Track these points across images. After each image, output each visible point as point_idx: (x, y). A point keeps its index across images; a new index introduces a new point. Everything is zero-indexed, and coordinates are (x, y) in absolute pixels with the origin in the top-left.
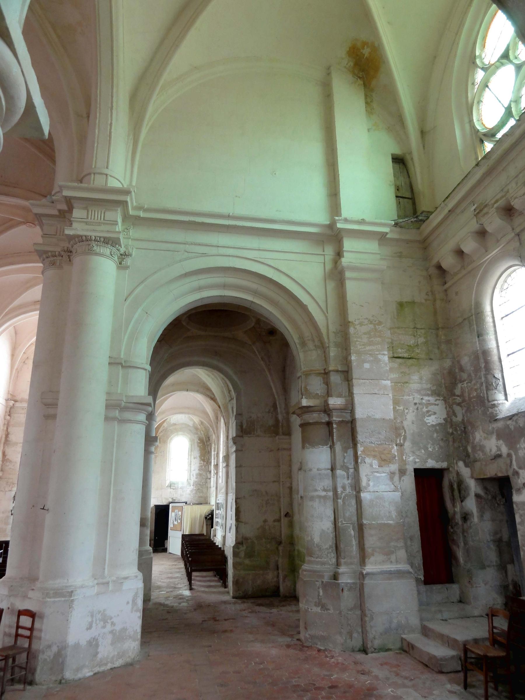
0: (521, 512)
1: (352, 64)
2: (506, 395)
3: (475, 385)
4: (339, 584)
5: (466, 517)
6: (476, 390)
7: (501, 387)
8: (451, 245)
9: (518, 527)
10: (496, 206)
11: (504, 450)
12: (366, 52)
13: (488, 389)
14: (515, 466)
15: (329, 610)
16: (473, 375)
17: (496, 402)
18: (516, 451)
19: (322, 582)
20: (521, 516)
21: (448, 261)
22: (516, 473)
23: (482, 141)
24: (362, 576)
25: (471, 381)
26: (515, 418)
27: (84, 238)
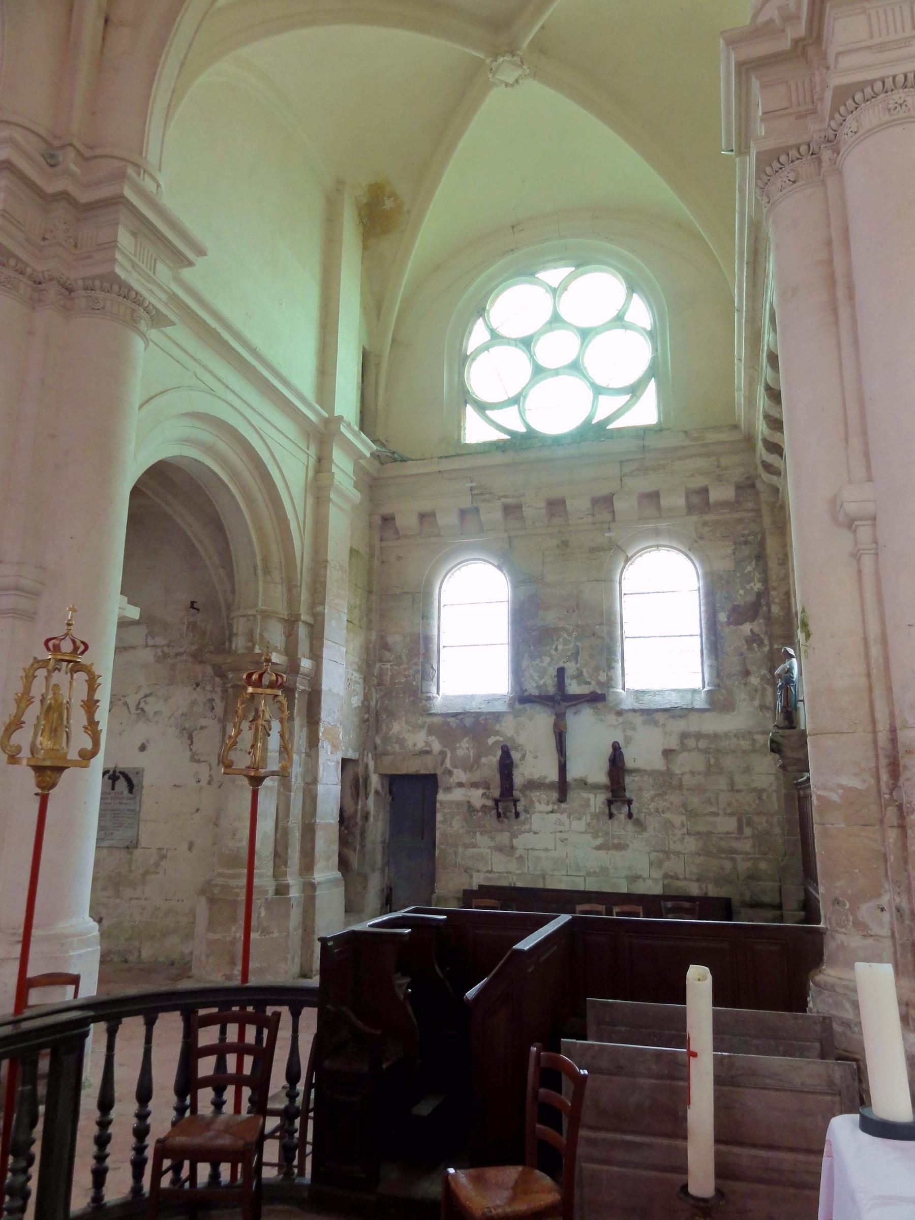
0: (446, 811)
1: (364, 200)
2: (438, 688)
3: (405, 670)
4: (290, 899)
5: (366, 817)
6: (406, 676)
7: (435, 680)
8: (425, 506)
9: (438, 825)
10: (503, 500)
11: (436, 747)
12: (389, 204)
13: (423, 678)
14: (448, 764)
15: (269, 933)
16: (404, 658)
17: (430, 695)
18: (453, 752)
19: (266, 899)
20: (445, 815)
21: (407, 520)
22: (450, 773)
23: (466, 403)
24: (313, 886)
25: (399, 664)
26: (460, 717)
27: (133, 294)
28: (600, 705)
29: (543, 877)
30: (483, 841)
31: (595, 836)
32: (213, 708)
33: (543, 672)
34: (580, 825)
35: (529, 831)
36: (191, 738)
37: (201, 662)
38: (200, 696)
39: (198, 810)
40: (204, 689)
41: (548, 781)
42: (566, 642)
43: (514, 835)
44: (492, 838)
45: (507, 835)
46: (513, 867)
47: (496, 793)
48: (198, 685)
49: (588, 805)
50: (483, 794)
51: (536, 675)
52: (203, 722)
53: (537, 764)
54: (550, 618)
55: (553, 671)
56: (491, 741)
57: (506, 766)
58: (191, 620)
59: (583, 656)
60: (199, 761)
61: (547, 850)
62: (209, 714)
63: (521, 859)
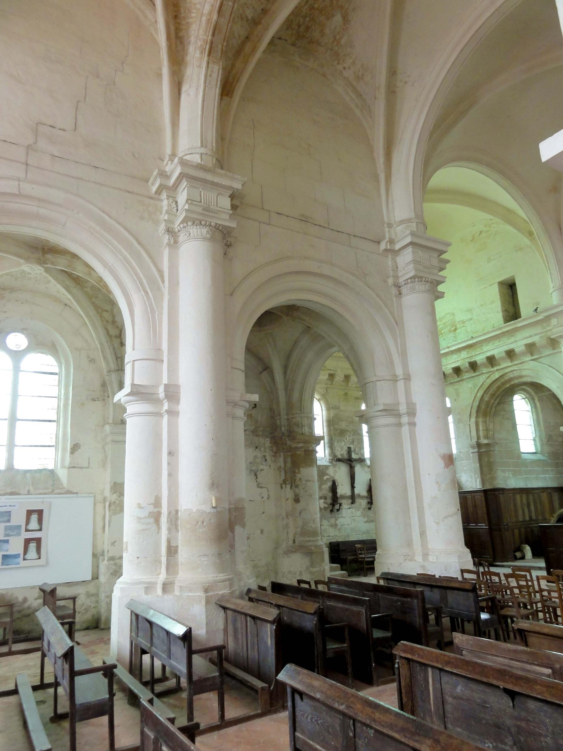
28: (362, 463)
29: (348, 536)
30: (325, 522)
31: (364, 517)
32: (266, 460)
33: (342, 448)
34: (359, 513)
35: (342, 517)
36: (256, 475)
37: (257, 436)
38: (259, 454)
39: (263, 513)
40: (260, 450)
41: (347, 495)
42: (349, 436)
43: (336, 519)
44: (329, 521)
45: (334, 519)
46: (337, 533)
47: (329, 501)
48: (257, 448)
49: (361, 505)
50: (324, 502)
51: (340, 449)
52: (261, 467)
53: (343, 489)
54: (343, 425)
55: (345, 448)
56: (325, 478)
57: (334, 488)
58: (249, 413)
59: (355, 443)
60: (261, 487)
61: (349, 525)
62: (264, 463)
63: (339, 529)
